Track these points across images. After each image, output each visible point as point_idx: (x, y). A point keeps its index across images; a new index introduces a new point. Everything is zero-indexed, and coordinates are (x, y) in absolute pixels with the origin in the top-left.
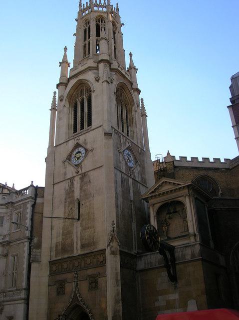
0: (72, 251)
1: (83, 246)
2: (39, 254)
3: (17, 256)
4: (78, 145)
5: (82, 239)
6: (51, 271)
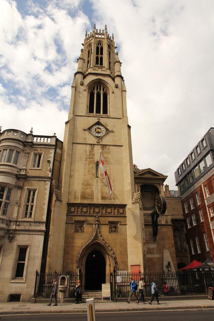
0: (92, 199)
1: (103, 198)
2: (59, 194)
3: (35, 192)
4: (98, 123)
5: (102, 192)
6: (68, 211)
